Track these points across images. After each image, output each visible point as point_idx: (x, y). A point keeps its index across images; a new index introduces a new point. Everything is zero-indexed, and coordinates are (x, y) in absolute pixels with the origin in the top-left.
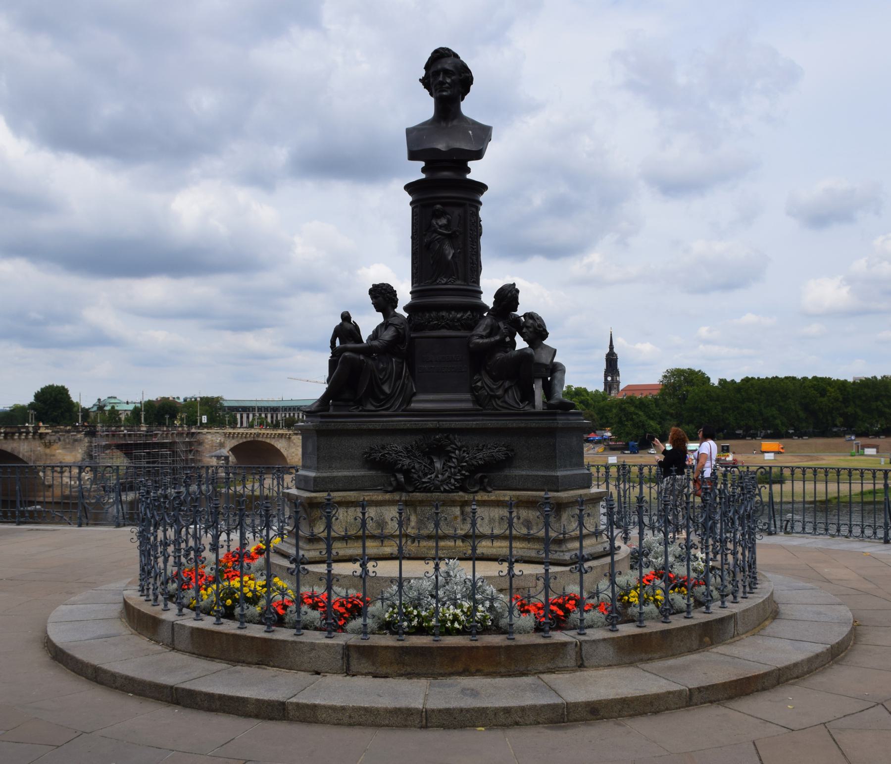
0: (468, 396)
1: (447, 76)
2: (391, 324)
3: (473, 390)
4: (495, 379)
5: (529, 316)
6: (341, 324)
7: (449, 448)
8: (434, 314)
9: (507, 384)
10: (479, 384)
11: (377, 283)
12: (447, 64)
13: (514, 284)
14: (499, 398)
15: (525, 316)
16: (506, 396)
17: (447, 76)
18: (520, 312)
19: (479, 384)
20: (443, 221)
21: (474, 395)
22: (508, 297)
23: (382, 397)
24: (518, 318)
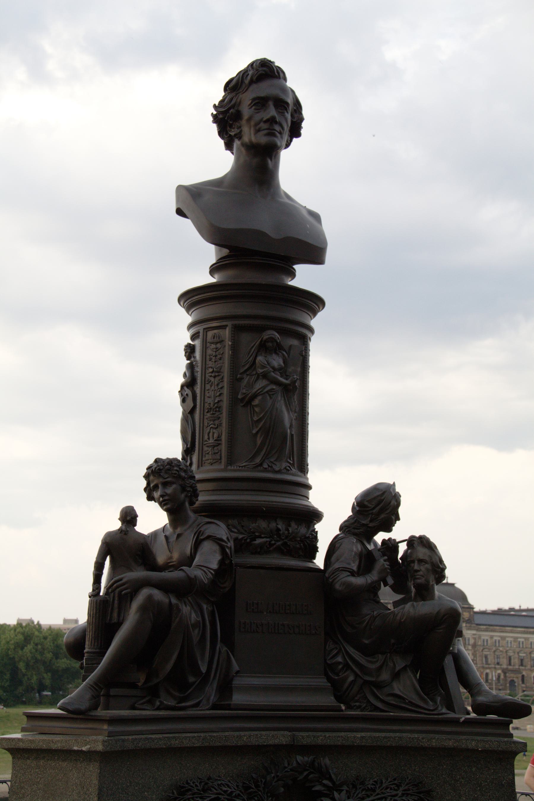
0: (322, 682)
1: (258, 111)
2: (209, 537)
3: (328, 670)
4: (365, 651)
5: (420, 544)
6: (120, 530)
7: (318, 788)
8: (263, 524)
9: (400, 663)
10: (339, 659)
11: (164, 457)
12: (264, 89)
13: (394, 483)
14: (379, 686)
15: (412, 541)
16: (395, 685)
17: (258, 111)
18: (400, 532)
19: (339, 659)
20: (277, 361)
21: (329, 679)
22: (377, 507)
23: (191, 679)
24: (391, 546)
